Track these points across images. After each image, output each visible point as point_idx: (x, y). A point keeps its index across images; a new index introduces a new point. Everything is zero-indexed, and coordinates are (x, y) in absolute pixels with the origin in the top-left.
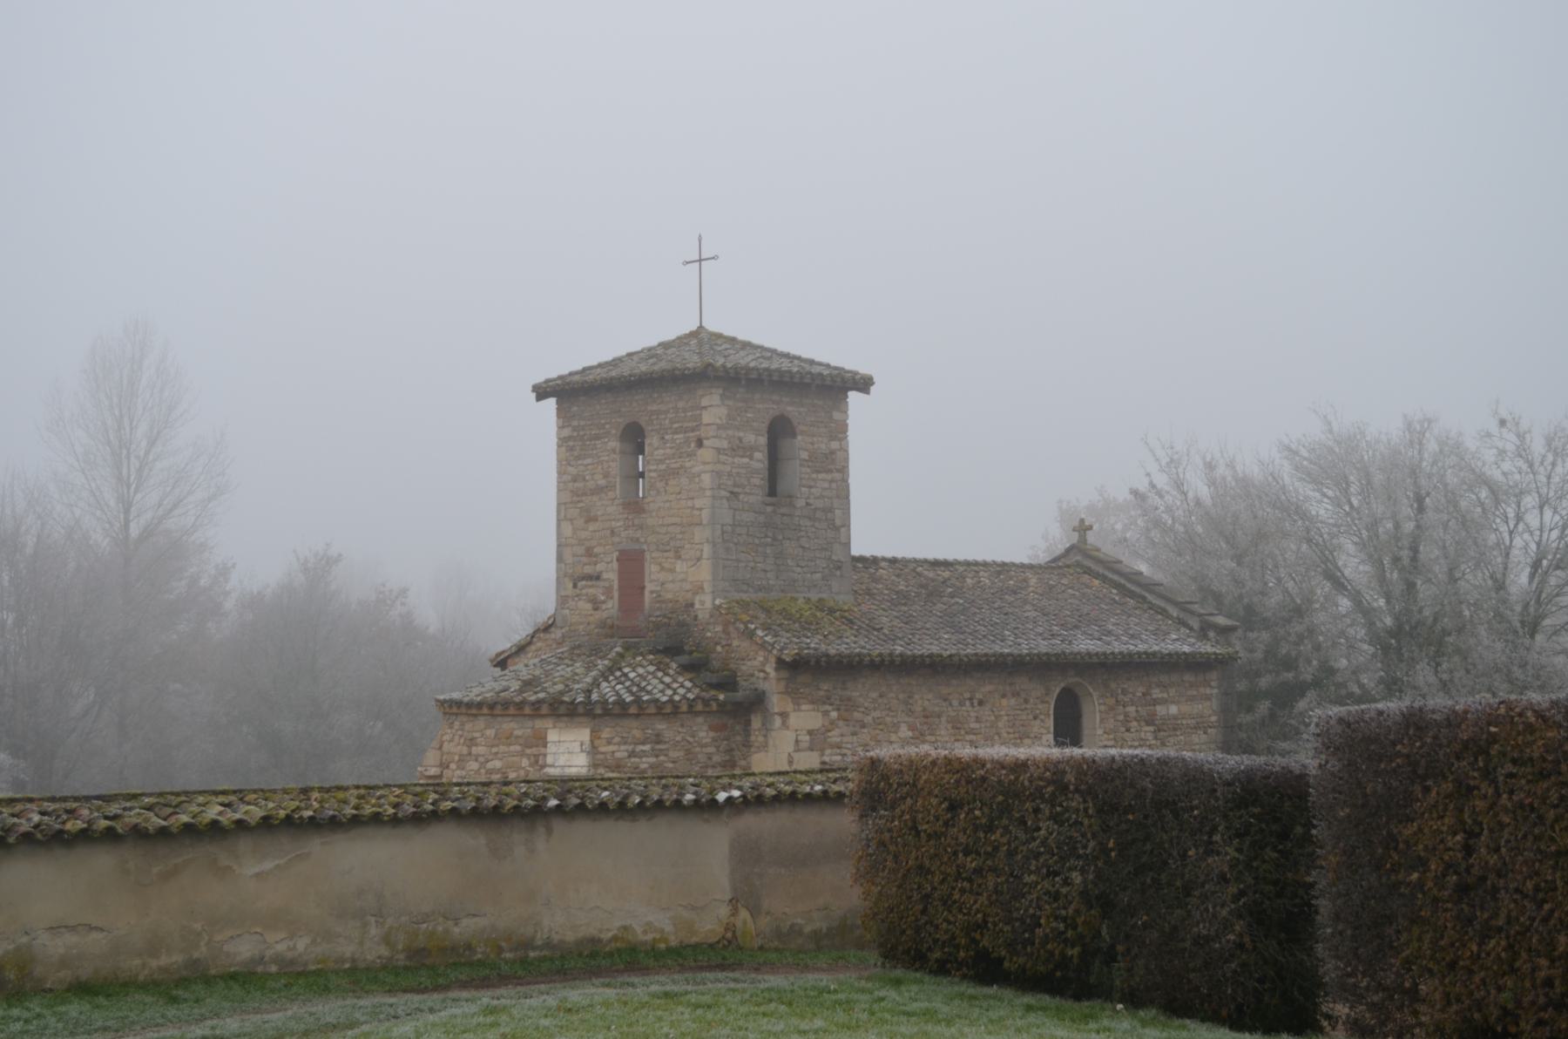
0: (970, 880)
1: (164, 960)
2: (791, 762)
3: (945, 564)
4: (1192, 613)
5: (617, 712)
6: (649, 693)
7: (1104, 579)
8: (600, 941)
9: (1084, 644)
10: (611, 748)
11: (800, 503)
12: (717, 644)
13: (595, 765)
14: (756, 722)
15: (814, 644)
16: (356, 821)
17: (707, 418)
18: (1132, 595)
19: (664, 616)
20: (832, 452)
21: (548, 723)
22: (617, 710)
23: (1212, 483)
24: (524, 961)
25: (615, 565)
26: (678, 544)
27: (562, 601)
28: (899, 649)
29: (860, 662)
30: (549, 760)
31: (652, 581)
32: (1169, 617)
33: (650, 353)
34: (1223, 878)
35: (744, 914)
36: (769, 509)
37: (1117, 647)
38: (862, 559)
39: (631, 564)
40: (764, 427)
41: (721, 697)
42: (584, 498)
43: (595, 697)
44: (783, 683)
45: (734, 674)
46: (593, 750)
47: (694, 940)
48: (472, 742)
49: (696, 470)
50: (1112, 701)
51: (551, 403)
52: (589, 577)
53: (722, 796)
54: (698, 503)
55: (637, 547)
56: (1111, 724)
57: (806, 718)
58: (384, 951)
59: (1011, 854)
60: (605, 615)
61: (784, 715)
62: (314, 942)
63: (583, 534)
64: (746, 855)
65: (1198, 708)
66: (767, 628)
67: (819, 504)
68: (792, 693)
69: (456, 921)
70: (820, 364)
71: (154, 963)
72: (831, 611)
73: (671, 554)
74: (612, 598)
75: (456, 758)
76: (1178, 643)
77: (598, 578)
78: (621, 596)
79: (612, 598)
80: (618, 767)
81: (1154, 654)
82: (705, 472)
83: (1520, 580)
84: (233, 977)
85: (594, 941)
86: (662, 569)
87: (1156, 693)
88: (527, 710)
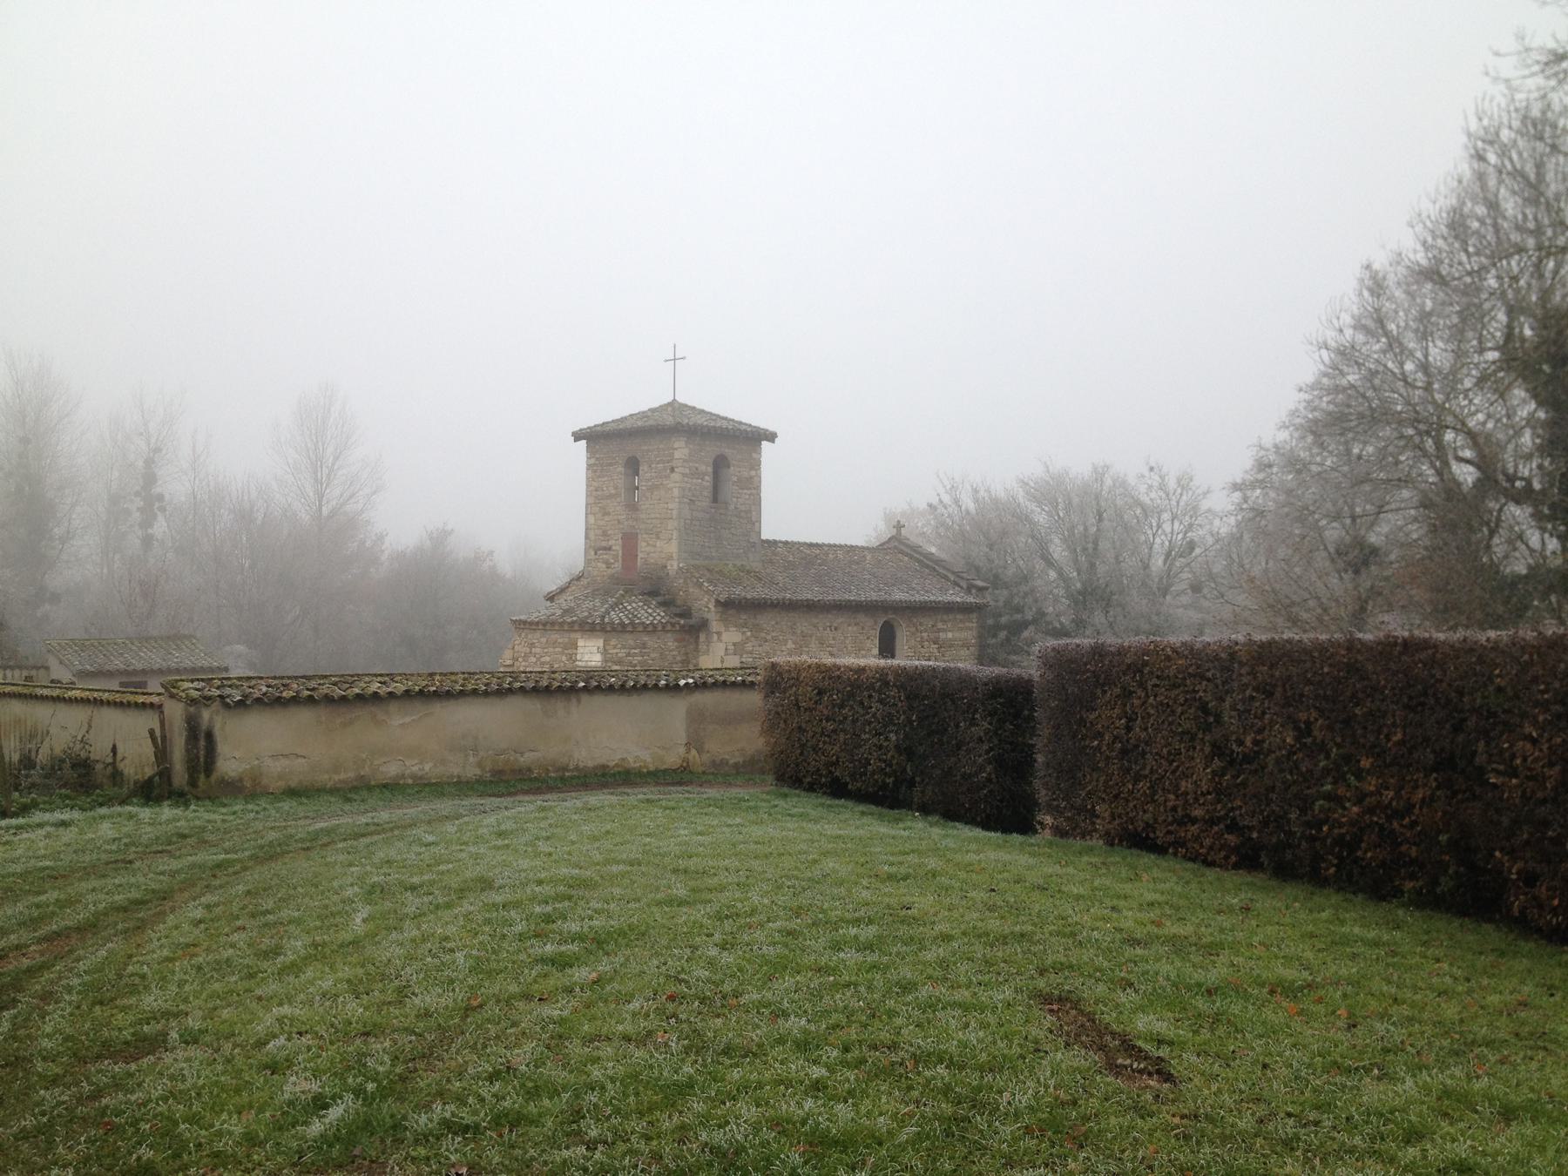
0: (829, 736)
1: (343, 776)
2: (722, 662)
3: (817, 545)
4: (962, 578)
5: (621, 629)
6: (638, 618)
7: (911, 557)
8: (608, 766)
9: (898, 596)
10: (615, 651)
11: (732, 507)
13: (606, 661)
14: (702, 637)
15: (738, 592)
16: (462, 694)
17: (677, 455)
18: (927, 567)
20: (751, 478)
21: (578, 635)
22: (620, 628)
23: (976, 501)
24: (562, 779)
27: (588, 562)
28: (788, 596)
29: (765, 603)
30: (579, 657)
32: (948, 580)
33: (643, 415)
34: (980, 740)
35: (694, 752)
36: (713, 510)
37: (918, 598)
38: (767, 541)
39: (630, 541)
40: (711, 461)
41: (682, 622)
43: (606, 620)
44: (719, 615)
45: (690, 609)
46: (605, 652)
47: (665, 767)
48: (532, 645)
50: (913, 629)
51: (583, 443)
52: (605, 549)
53: (682, 682)
54: (670, 506)
56: (913, 642)
57: (732, 636)
58: (478, 772)
59: (854, 721)
60: (613, 571)
61: (719, 634)
62: (435, 765)
64: (696, 718)
65: (964, 635)
66: (710, 581)
67: (743, 508)
68: (725, 621)
69: (522, 754)
70: (746, 424)
71: (336, 778)
72: (748, 572)
73: (654, 536)
76: (955, 596)
78: (623, 560)
80: (619, 662)
81: (939, 602)
83: (1158, 563)
84: (385, 786)
85: (604, 767)
86: (648, 545)
87: (940, 625)
88: (566, 628)
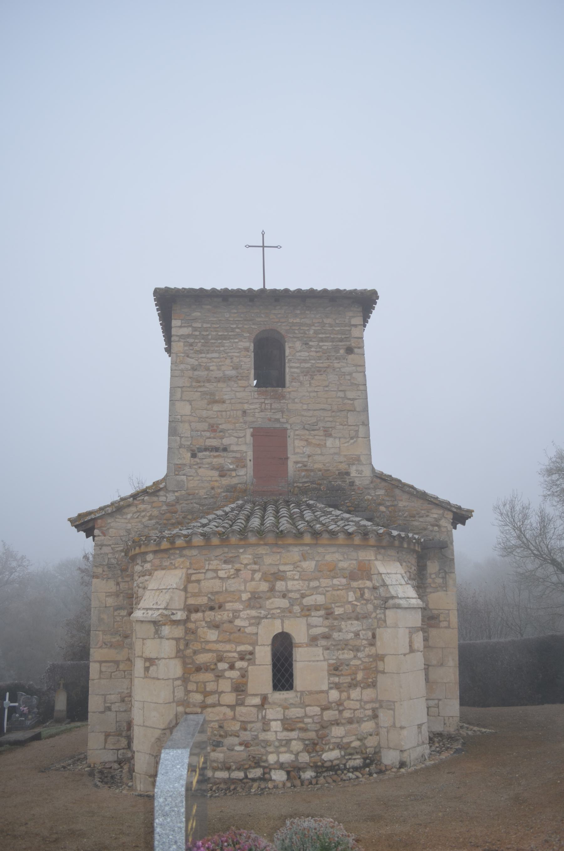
12: (380, 504)
19: (312, 483)
25: (249, 439)
26: (328, 424)
31: (295, 454)
42: (207, 384)
48: (279, 576)
49: (347, 370)
52: (216, 449)
54: (350, 395)
55: (278, 425)
60: (235, 481)
63: (204, 413)
73: (322, 433)
74: (245, 466)
75: (245, 597)
77: (225, 450)
79: (245, 466)
82: (357, 372)
86: (309, 443)
